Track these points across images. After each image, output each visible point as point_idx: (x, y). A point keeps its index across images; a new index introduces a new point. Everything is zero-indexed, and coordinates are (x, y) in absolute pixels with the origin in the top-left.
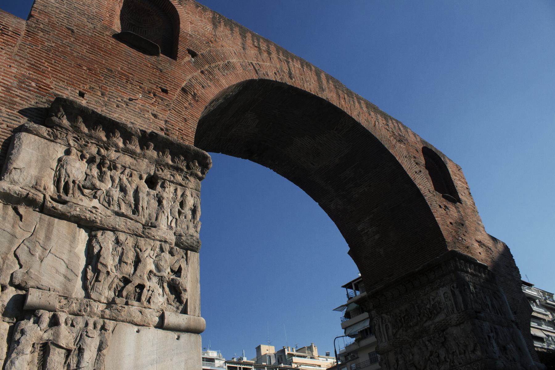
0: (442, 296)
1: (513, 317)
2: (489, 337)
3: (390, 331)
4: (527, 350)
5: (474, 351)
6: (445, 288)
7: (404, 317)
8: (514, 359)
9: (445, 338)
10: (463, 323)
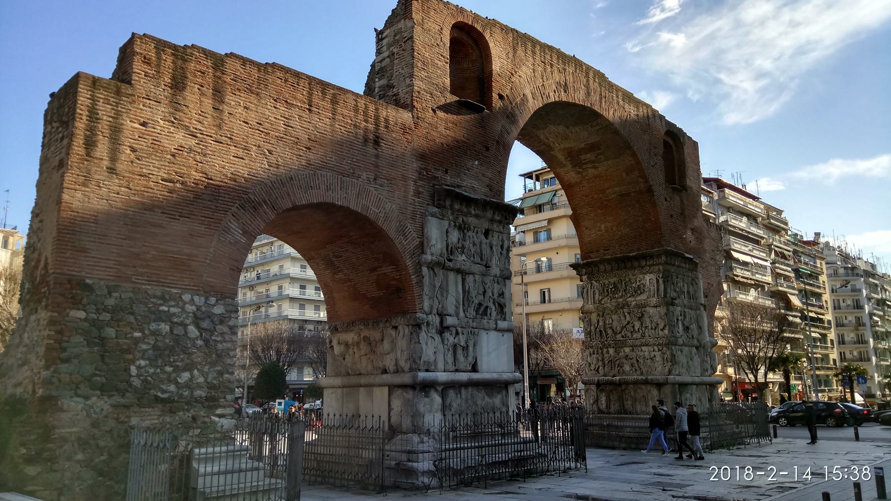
0: (648, 281)
1: (703, 300)
2: (678, 319)
3: (597, 296)
4: (706, 328)
5: (662, 330)
6: (652, 275)
7: (611, 289)
8: (693, 336)
9: (643, 315)
10: (660, 306)
